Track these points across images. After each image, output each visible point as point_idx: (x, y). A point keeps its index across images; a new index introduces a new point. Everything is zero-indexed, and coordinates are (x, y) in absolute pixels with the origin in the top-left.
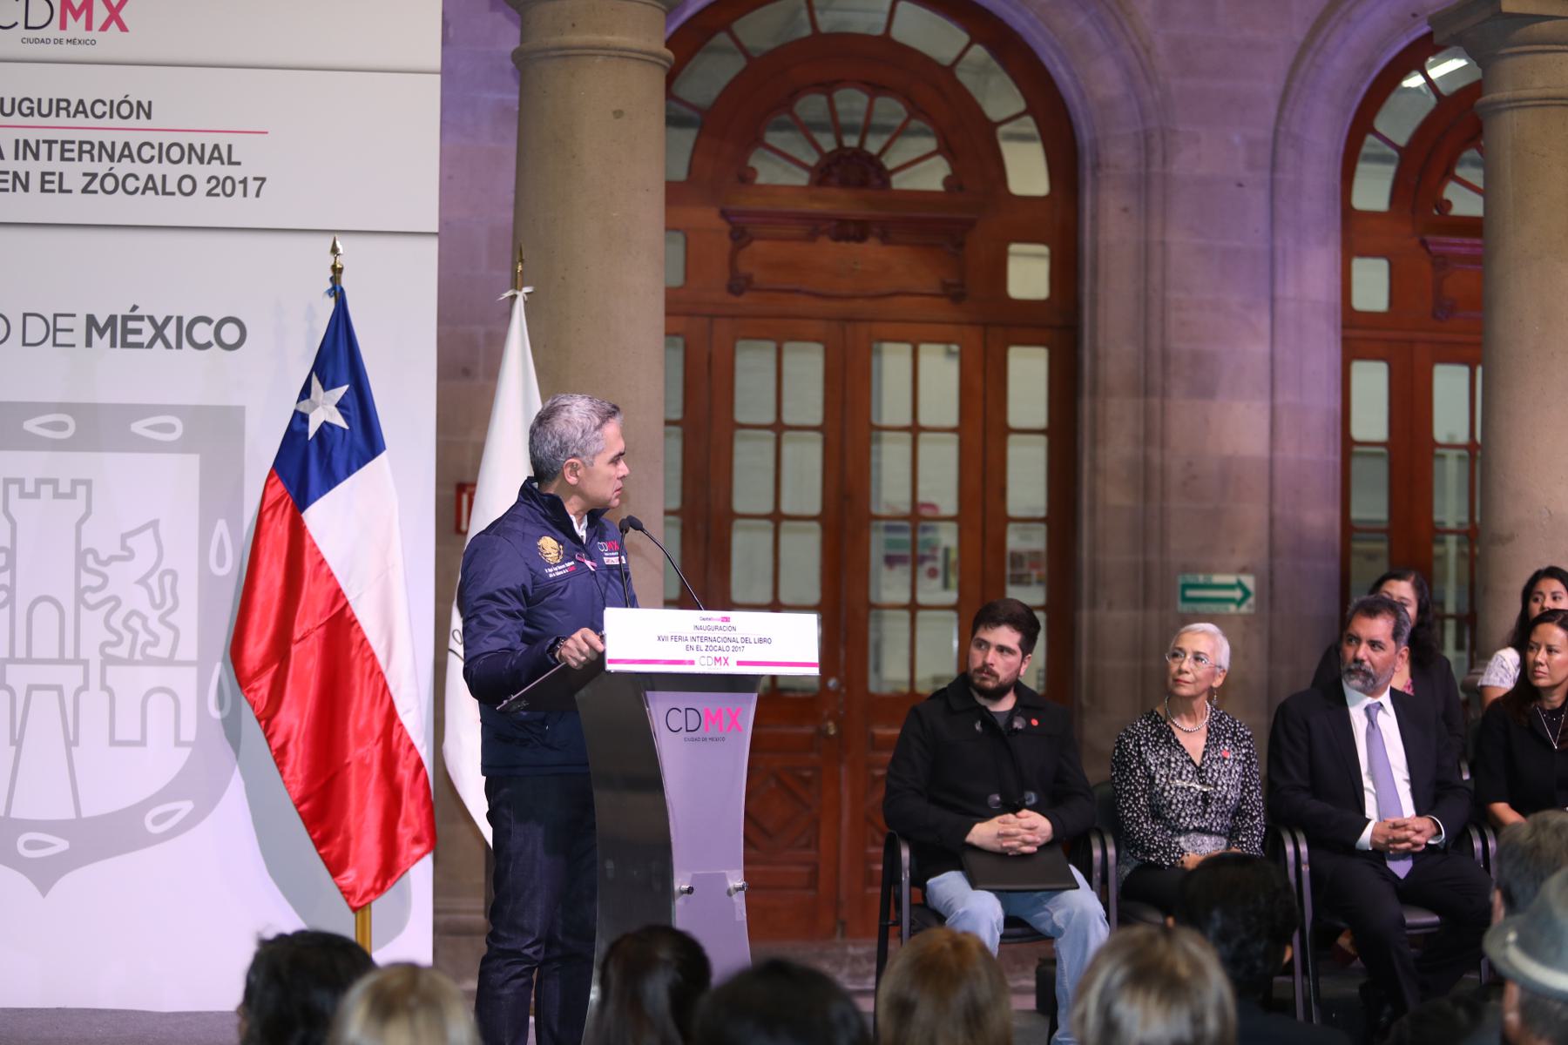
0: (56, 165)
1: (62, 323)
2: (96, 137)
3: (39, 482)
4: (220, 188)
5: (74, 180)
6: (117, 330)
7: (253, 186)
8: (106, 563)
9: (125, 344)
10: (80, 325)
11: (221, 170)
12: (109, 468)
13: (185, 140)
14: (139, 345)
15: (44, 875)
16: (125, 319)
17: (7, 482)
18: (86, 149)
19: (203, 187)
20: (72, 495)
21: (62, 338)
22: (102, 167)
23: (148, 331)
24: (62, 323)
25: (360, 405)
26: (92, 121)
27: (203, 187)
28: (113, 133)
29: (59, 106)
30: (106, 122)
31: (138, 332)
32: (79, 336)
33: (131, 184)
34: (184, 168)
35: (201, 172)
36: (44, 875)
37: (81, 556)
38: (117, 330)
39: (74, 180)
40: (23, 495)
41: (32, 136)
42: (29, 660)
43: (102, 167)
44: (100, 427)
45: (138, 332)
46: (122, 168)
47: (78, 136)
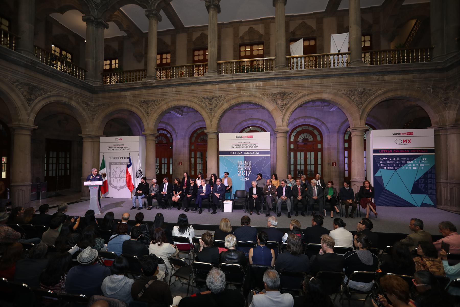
6: (122, 158)
12: (122, 166)
15: (119, 190)
25: (131, 163)
36: (119, 190)
38: (122, 158)
44: (121, 164)
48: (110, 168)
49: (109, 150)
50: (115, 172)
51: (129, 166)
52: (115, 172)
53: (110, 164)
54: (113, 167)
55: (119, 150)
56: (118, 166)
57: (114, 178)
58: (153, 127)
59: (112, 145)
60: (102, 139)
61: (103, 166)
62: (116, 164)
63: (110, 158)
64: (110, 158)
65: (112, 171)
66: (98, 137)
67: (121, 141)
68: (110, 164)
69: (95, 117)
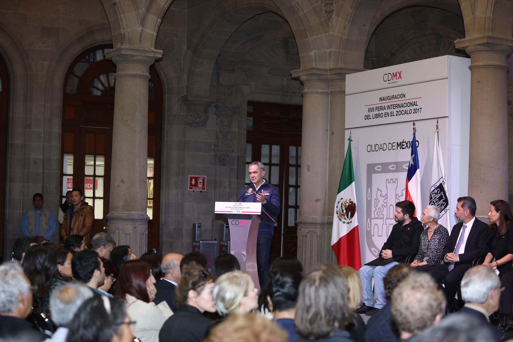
0: (392, 110)
1: (394, 144)
2: (397, 103)
3: (391, 179)
4: (416, 111)
5: (395, 113)
7: (420, 110)
8: (399, 197)
9: (403, 148)
10: (395, 144)
11: (415, 107)
13: (410, 101)
14: (404, 148)
16: (403, 142)
17: (387, 180)
18: (398, 106)
19: (413, 111)
20: (395, 182)
21: (394, 148)
22: (398, 110)
23: (405, 145)
24: (394, 144)
25: (415, 159)
26: (397, 100)
27: (413, 111)
28: (400, 102)
29: (394, 97)
30: (399, 99)
31: (404, 145)
32: (395, 148)
33: (403, 112)
34: (410, 108)
35: (412, 108)
37: (396, 195)
39: (395, 113)
40: (389, 183)
41: (389, 104)
42: (389, 219)
43: (398, 110)
45: (404, 145)
46: (402, 109)
47: (395, 103)
48: (369, 184)
49: (367, 117)
50: (381, 199)
51: (412, 171)
52: (381, 199)
53: (371, 169)
54: (379, 180)
55: (392, 114)
56: (389, 176)
57: (380, 222)
58: (489, 14)
59: (374, 99)
60: (354, 81)
61: (347, 178)
62: (385, 168)
63: (373, 148)
64: (373, 148)
65: (374, 197)
66: (340, 75)
67: (400, 82)
68: (371, 169)
69: (335, 7)
